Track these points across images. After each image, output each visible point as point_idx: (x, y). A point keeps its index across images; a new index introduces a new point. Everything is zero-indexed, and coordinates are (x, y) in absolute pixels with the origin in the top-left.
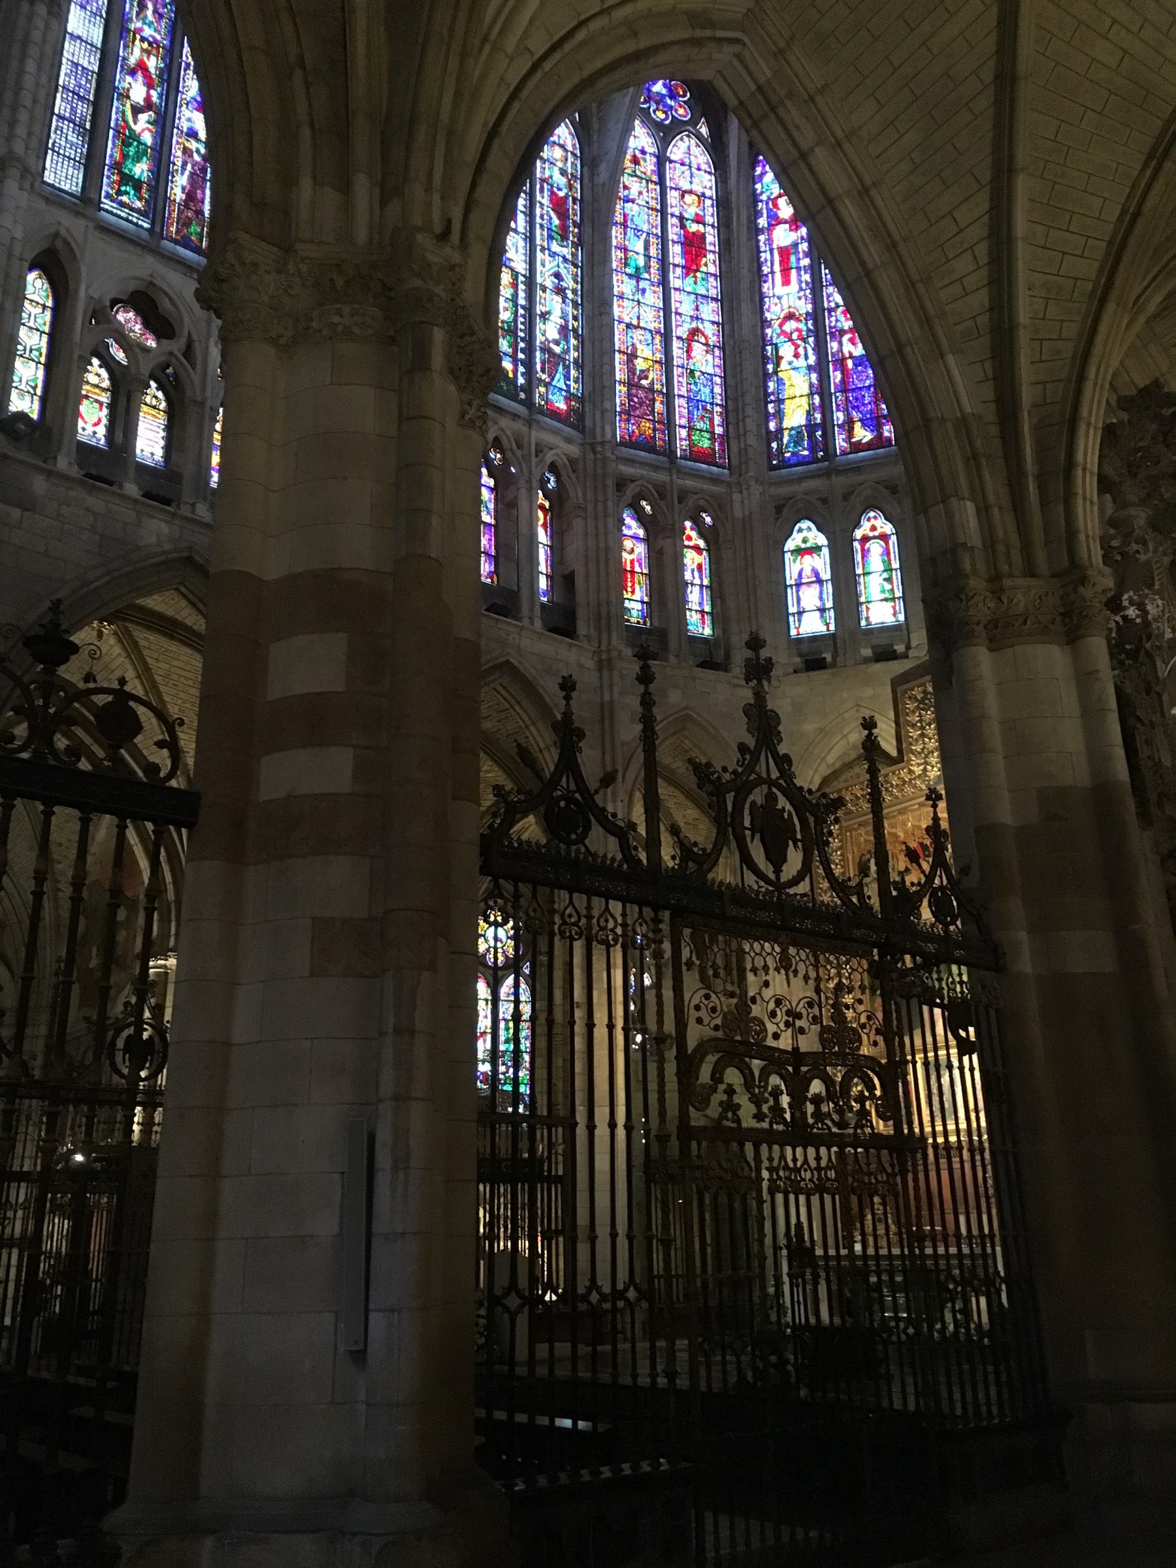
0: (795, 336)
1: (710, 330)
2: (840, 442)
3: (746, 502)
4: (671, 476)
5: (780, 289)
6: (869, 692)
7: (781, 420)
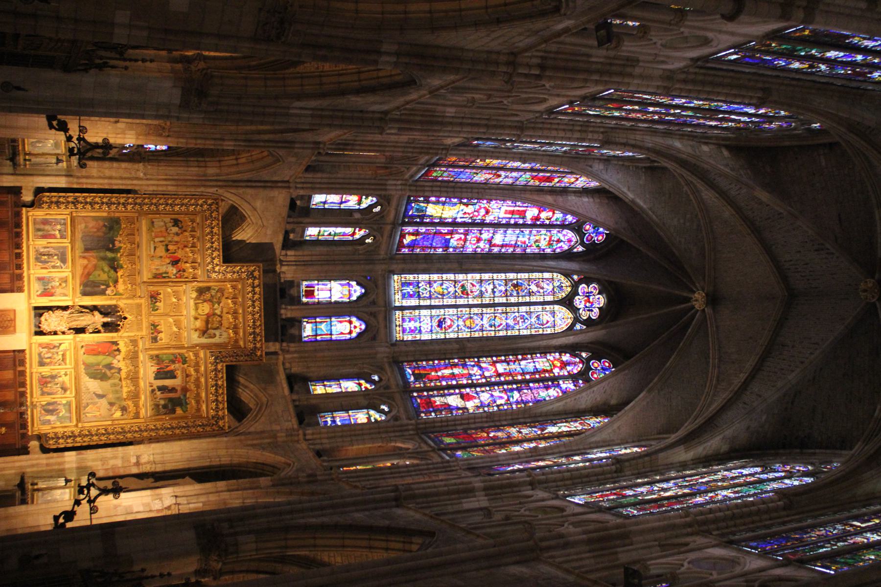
0: (476, 213)
1: (498, 180)
2: (410, 229)
3: (394, 187)
4: (421, 165)
5: (504, 209)
6: (269, 232)
7: (434, 203)
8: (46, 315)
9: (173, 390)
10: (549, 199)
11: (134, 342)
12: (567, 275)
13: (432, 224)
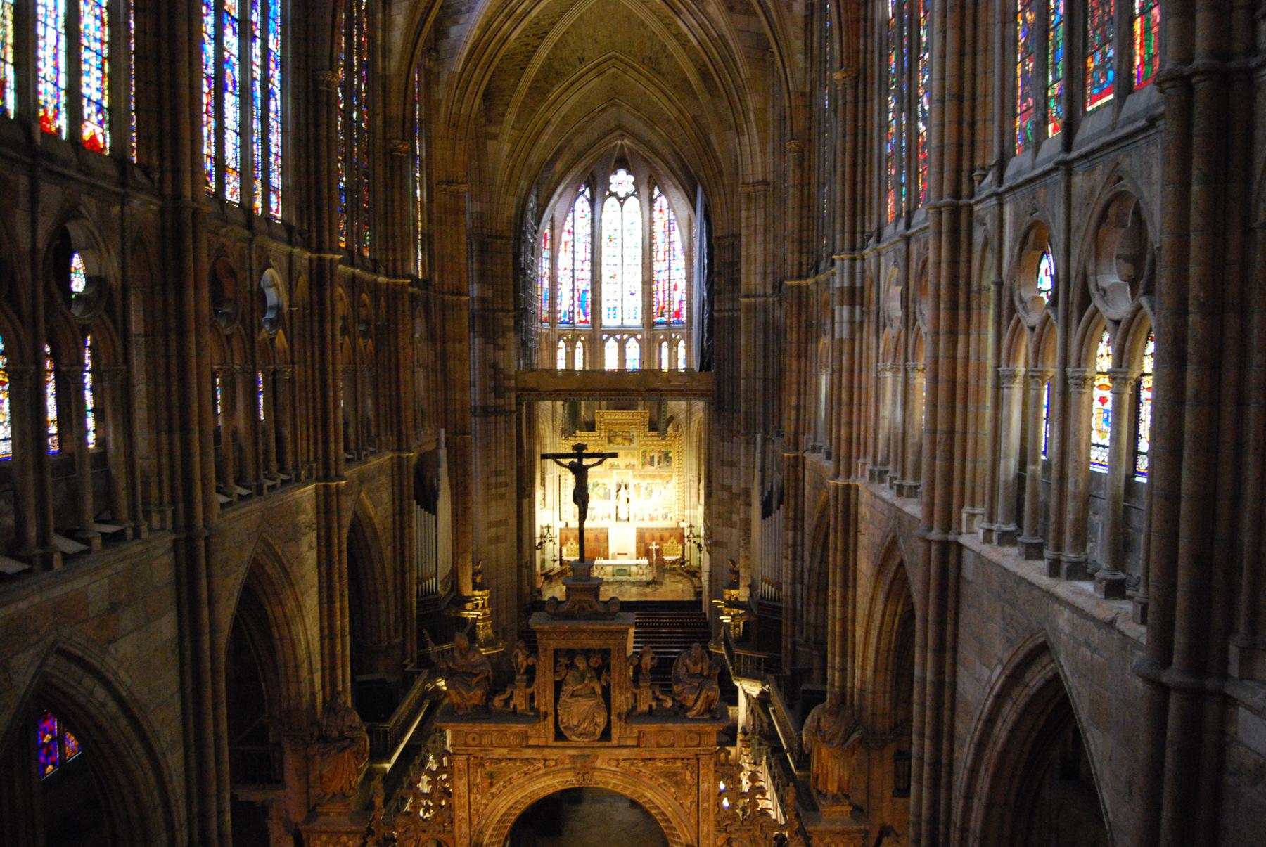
2: (576, 320)
8: (619, 516)
9: (660, 457)
10: (557, 231)
11: (634, 476)
12: (604, 199)
13: (573, 305)
